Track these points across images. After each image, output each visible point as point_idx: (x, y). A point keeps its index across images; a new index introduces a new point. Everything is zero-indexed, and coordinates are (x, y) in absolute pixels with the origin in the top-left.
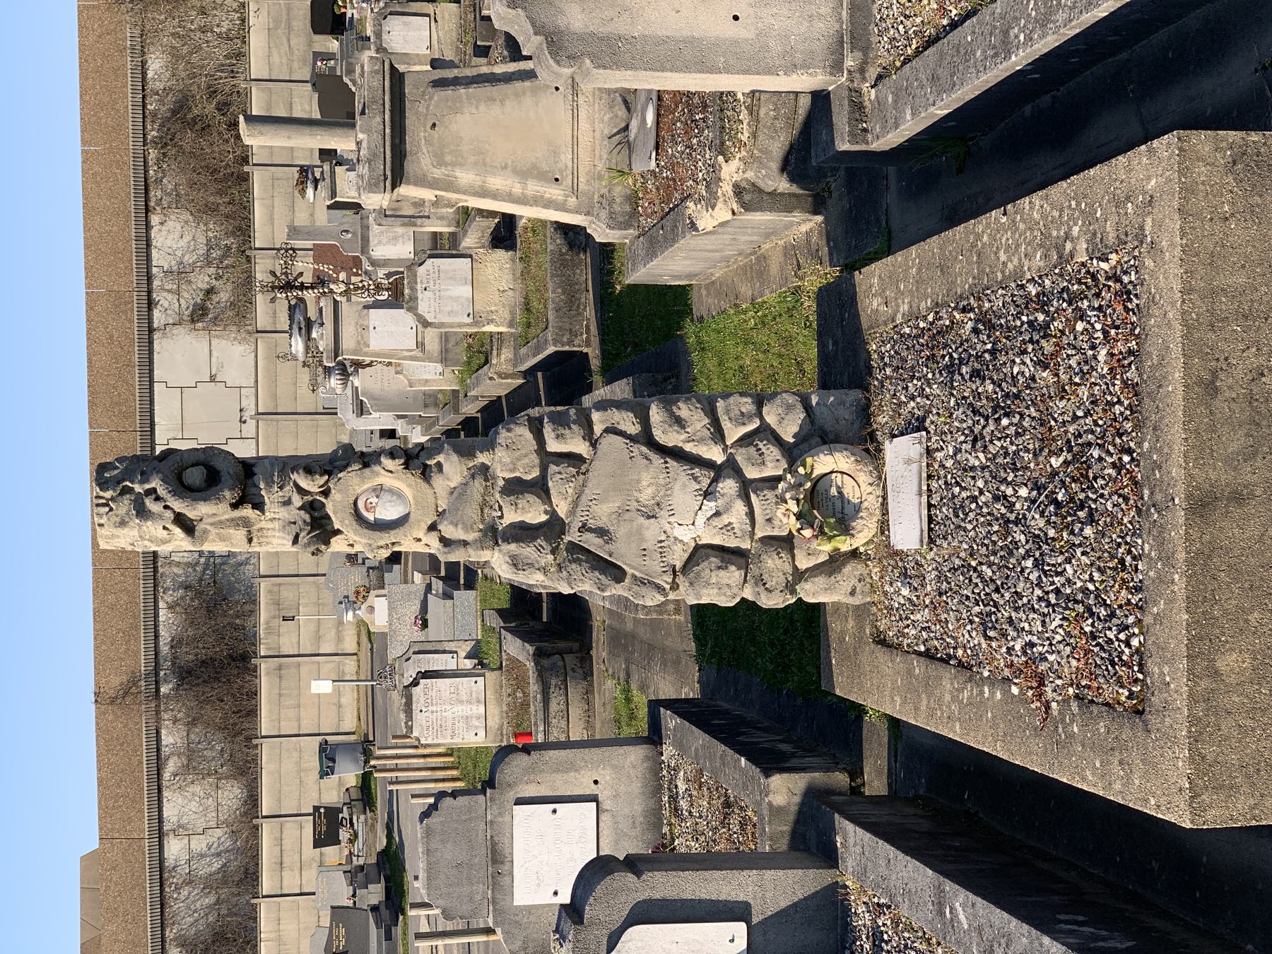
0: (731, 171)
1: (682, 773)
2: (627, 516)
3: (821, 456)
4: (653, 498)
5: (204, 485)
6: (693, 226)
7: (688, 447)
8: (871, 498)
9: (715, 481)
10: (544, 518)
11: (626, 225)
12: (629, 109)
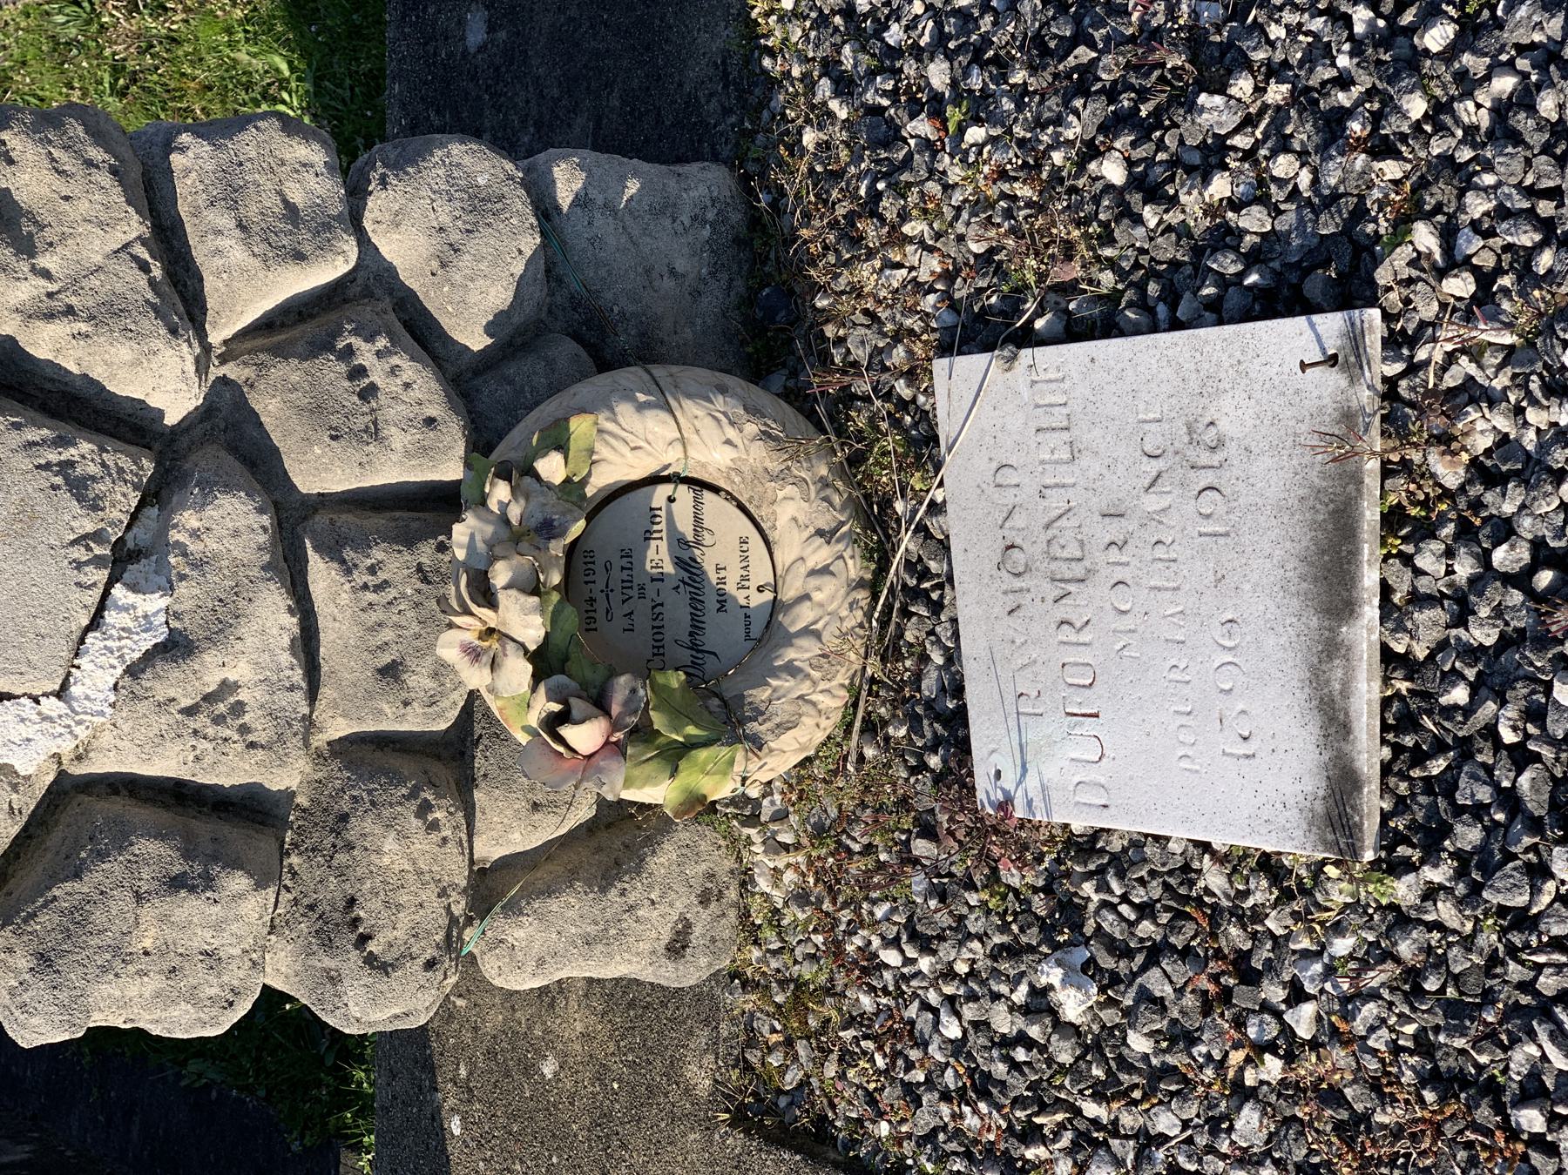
3: (625, 410)
7: (47, 343)
9: (156, 495)
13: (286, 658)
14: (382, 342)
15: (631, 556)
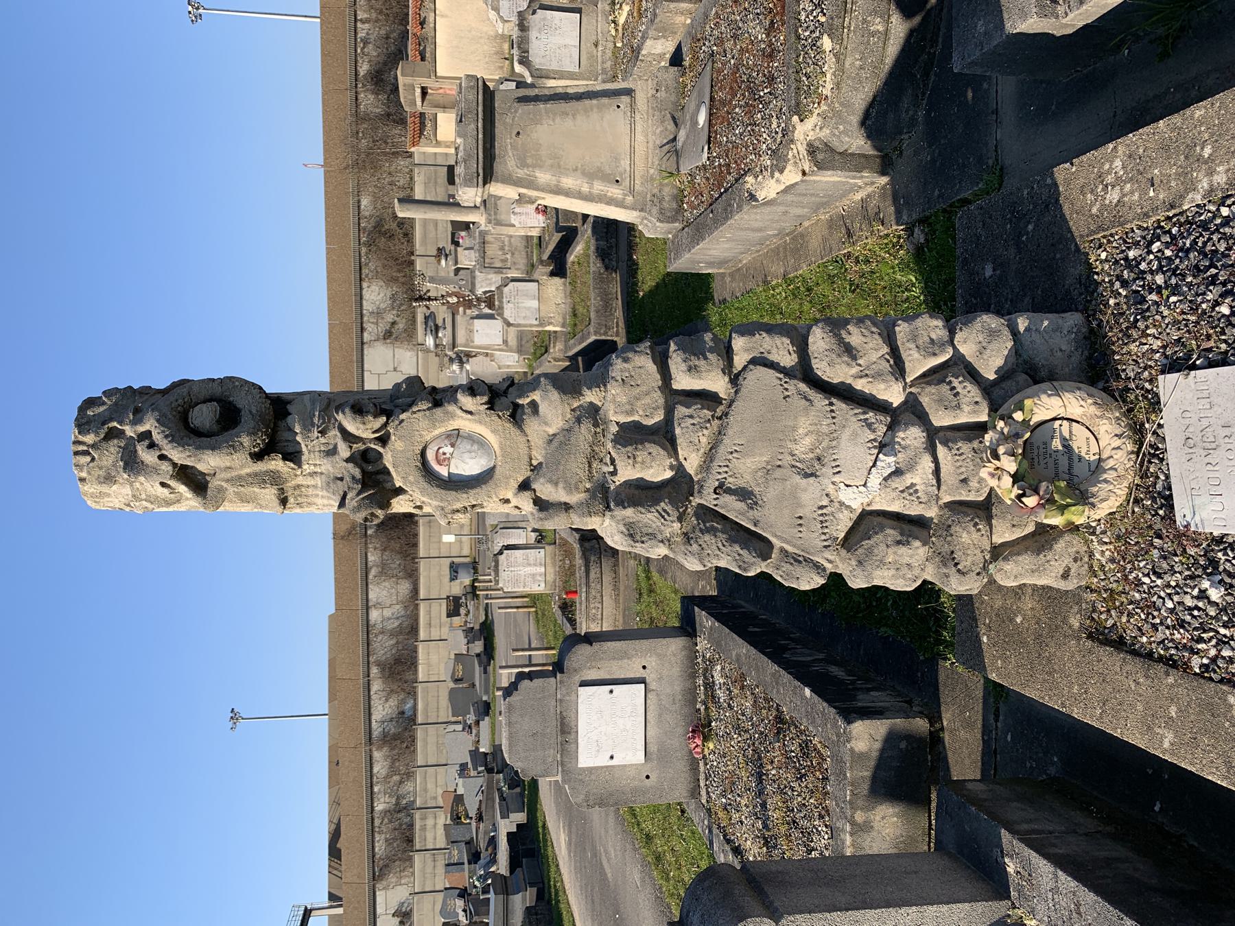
0: (805, 130)
1: (719, 667)
2: (778, 473)
3: (1044, 397)
4: (812, 451)
5: (215, 428)
6: (752, 197)
7: (860, 385)
8: (1119, 455)
9: (891, 427)
10: (669, 474)
11: (673, 220)
12: (676, 124)
13: (931, 476)
14: (961, 379)
15: (1046, 444)
